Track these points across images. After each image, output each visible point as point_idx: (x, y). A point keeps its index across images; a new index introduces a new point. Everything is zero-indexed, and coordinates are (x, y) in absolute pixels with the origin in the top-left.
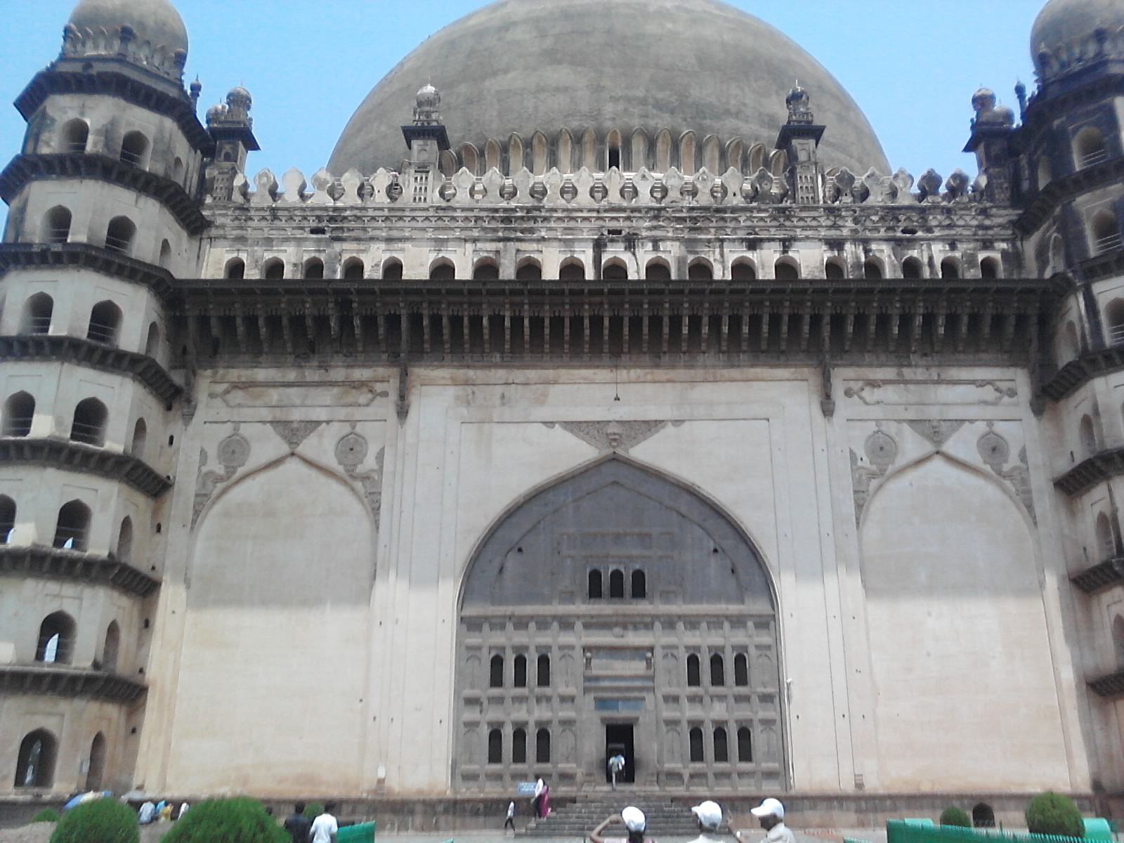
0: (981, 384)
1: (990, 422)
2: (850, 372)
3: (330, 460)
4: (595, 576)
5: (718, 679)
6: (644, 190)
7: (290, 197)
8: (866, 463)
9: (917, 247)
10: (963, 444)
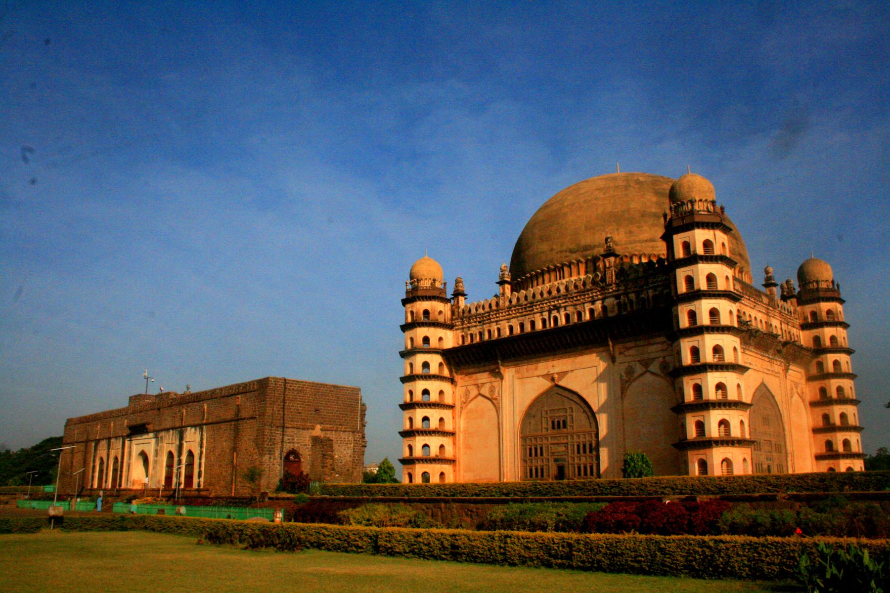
0: (662, 343)
1: (664, 358)
2: (620, 346)
3: (488, 395)
4: (553, 422)
5: (585, 452)
6: (562, 289)
7: (473, 311)
8: (624, 377)
9: (645, 292)
10: (655, 367)
